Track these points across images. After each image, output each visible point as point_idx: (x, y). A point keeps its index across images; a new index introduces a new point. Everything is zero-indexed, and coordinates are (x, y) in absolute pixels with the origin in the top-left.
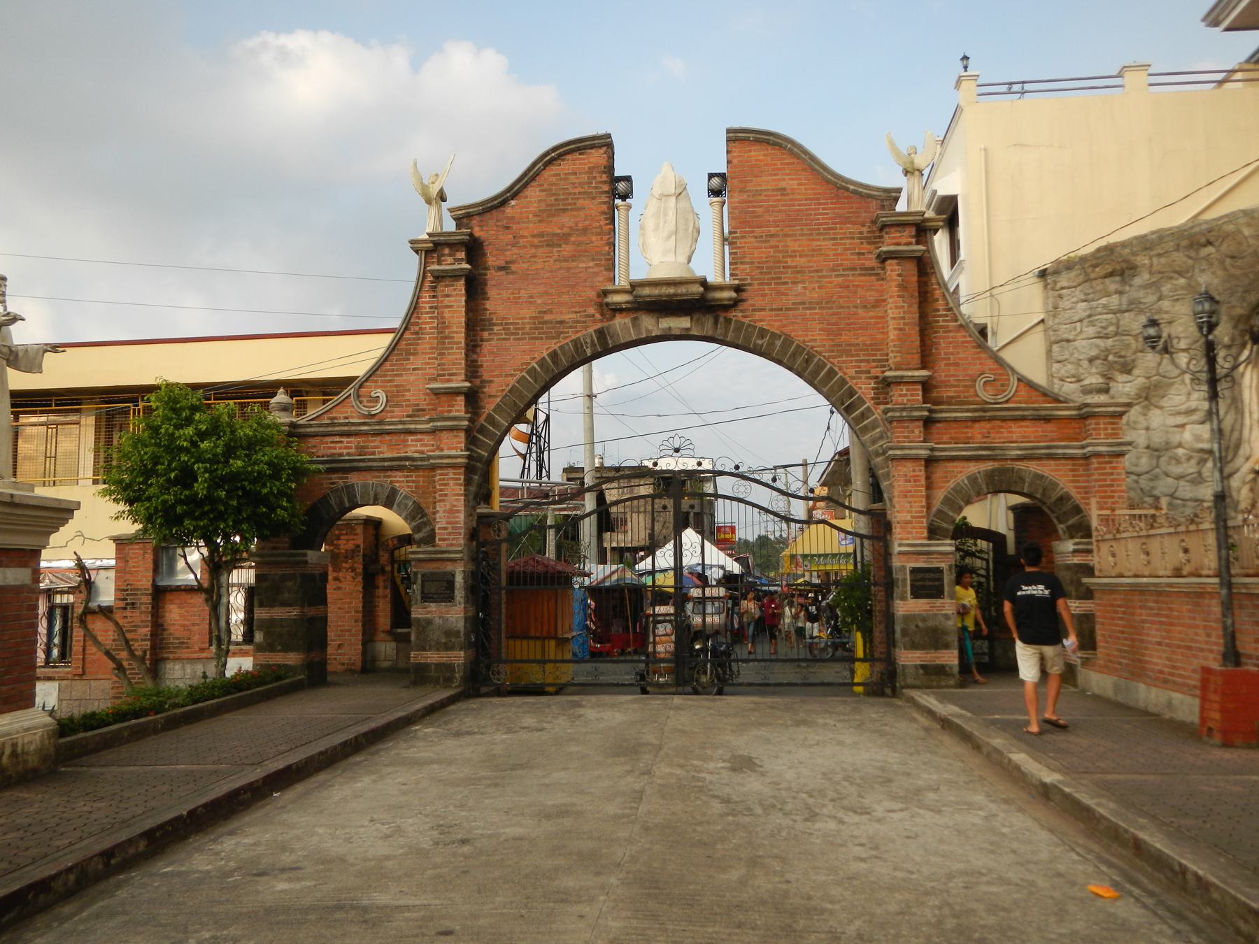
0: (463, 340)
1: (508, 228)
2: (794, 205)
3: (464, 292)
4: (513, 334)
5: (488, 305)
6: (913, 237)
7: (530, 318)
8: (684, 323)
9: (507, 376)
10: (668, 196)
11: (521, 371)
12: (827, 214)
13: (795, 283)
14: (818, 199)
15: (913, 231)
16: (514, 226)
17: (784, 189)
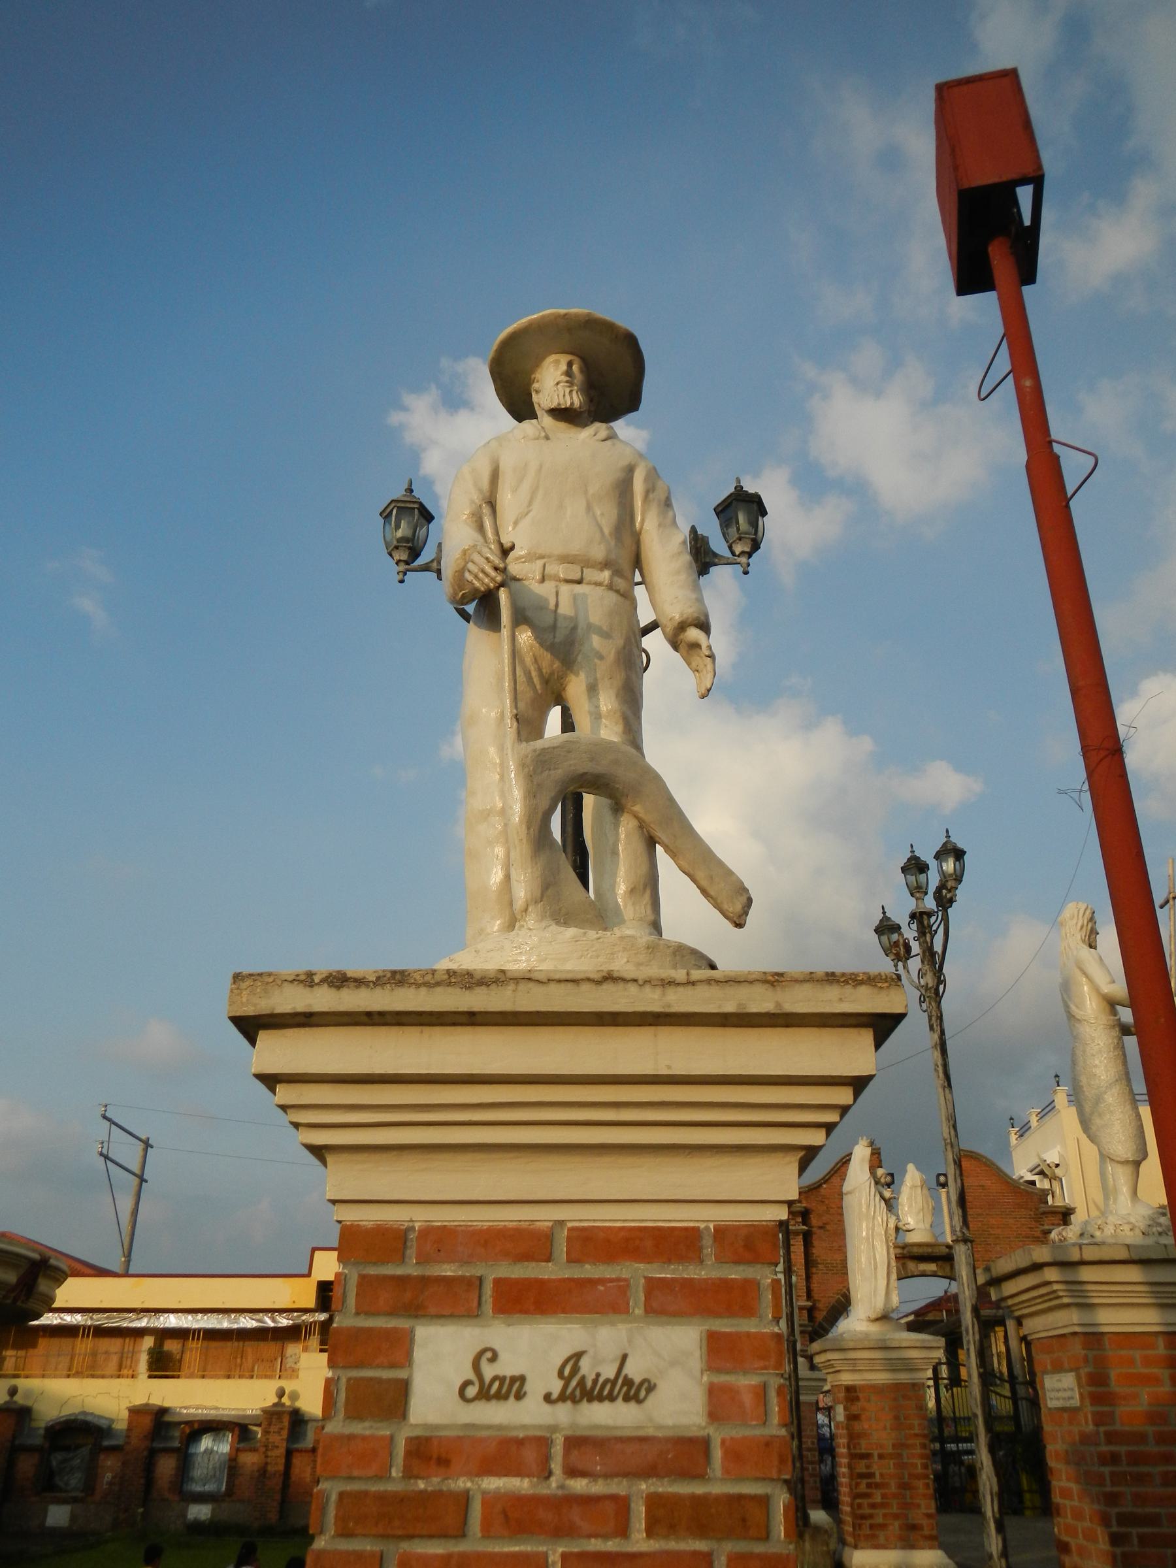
0: (804, 1274)
1: (823, 1202)
2: (990, 1196)
3: (802, 1243)
4: (831, 1270)
5: (814, 1251)
6: (1061, 1220)
7: (841, 1260)
8: (932, 1267)
9: (829, 1297)
10: (916, 1187)
11: (838, 1294)
12: (1009, 1202)
13: (996, 1244)
14: (1004, 1193)
15: (1061, 1217)
16: (827, 1202)
17: (983, 1186)
